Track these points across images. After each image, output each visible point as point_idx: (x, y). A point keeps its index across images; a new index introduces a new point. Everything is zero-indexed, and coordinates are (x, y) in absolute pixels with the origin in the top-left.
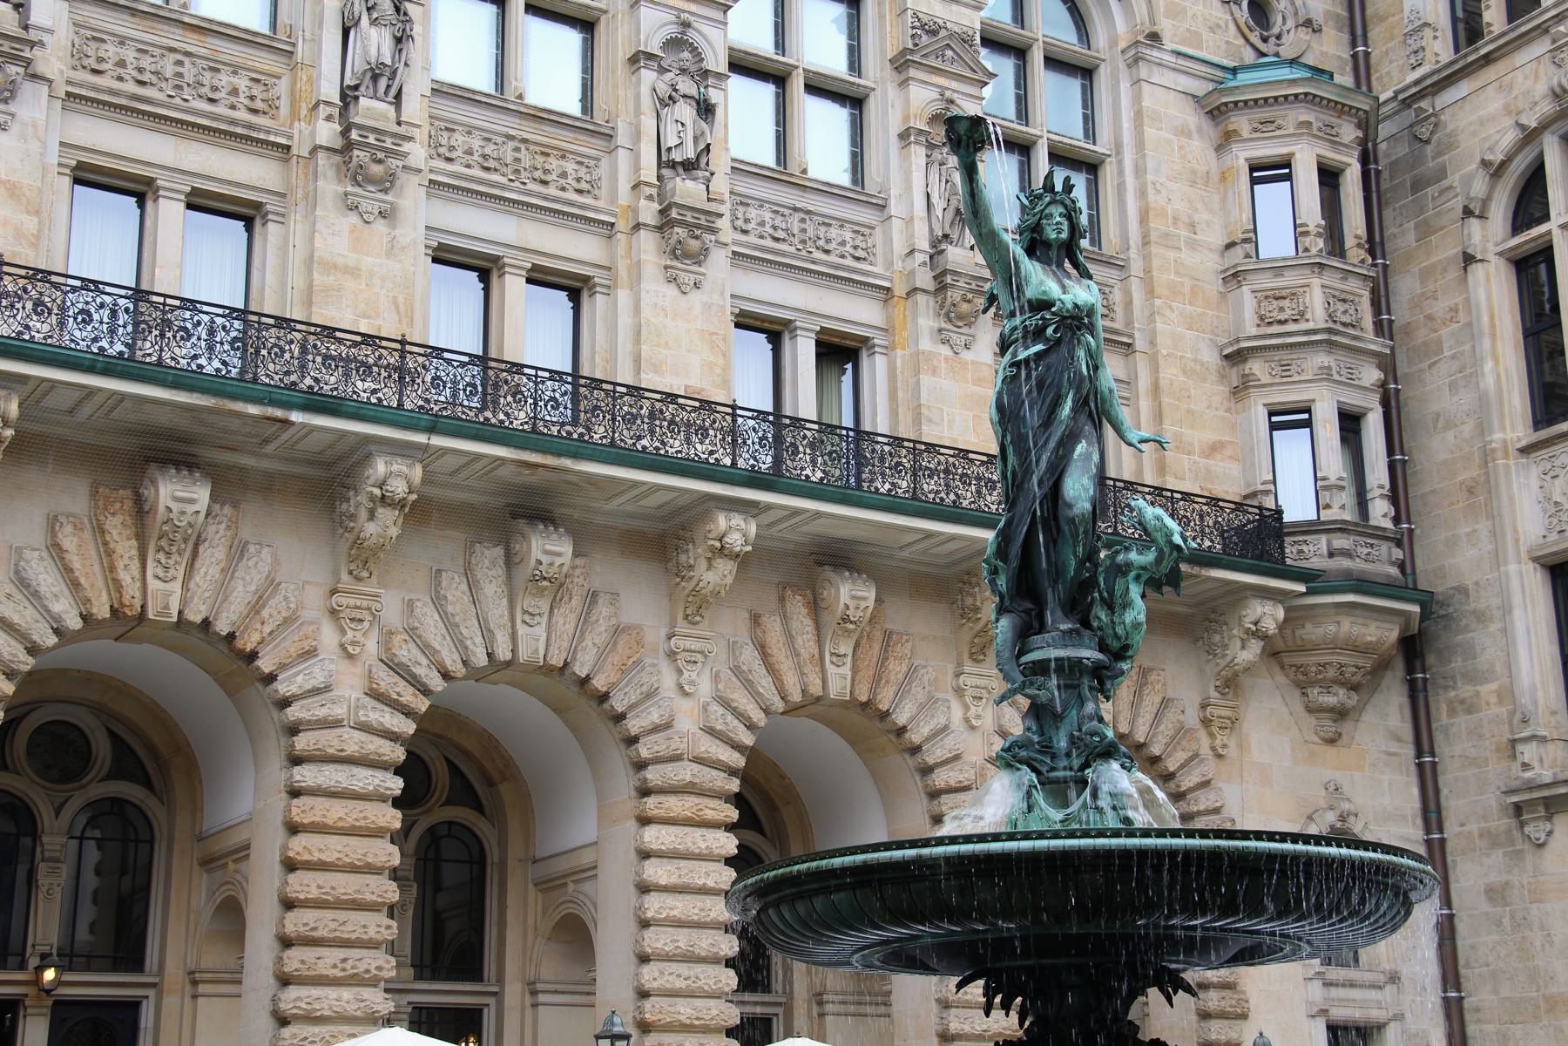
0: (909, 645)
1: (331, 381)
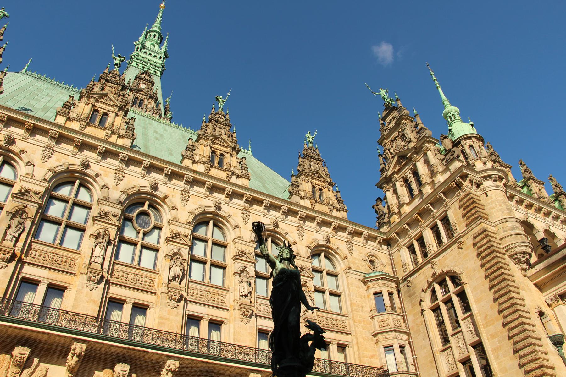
1: (159, 342)
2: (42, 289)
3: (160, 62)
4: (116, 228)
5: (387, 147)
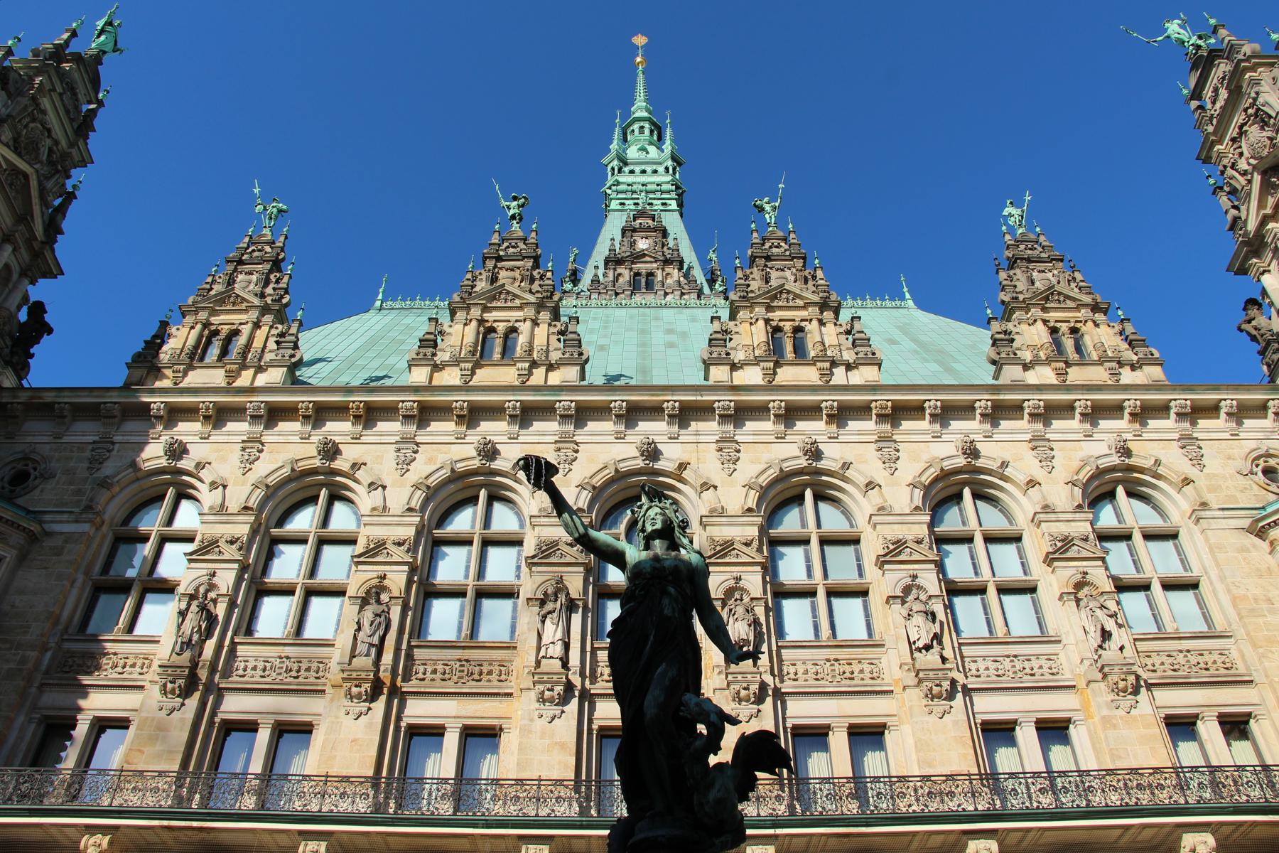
2: (451, 741)
3: (669, 178)
4: (759, 568)
5: (1225, 161)
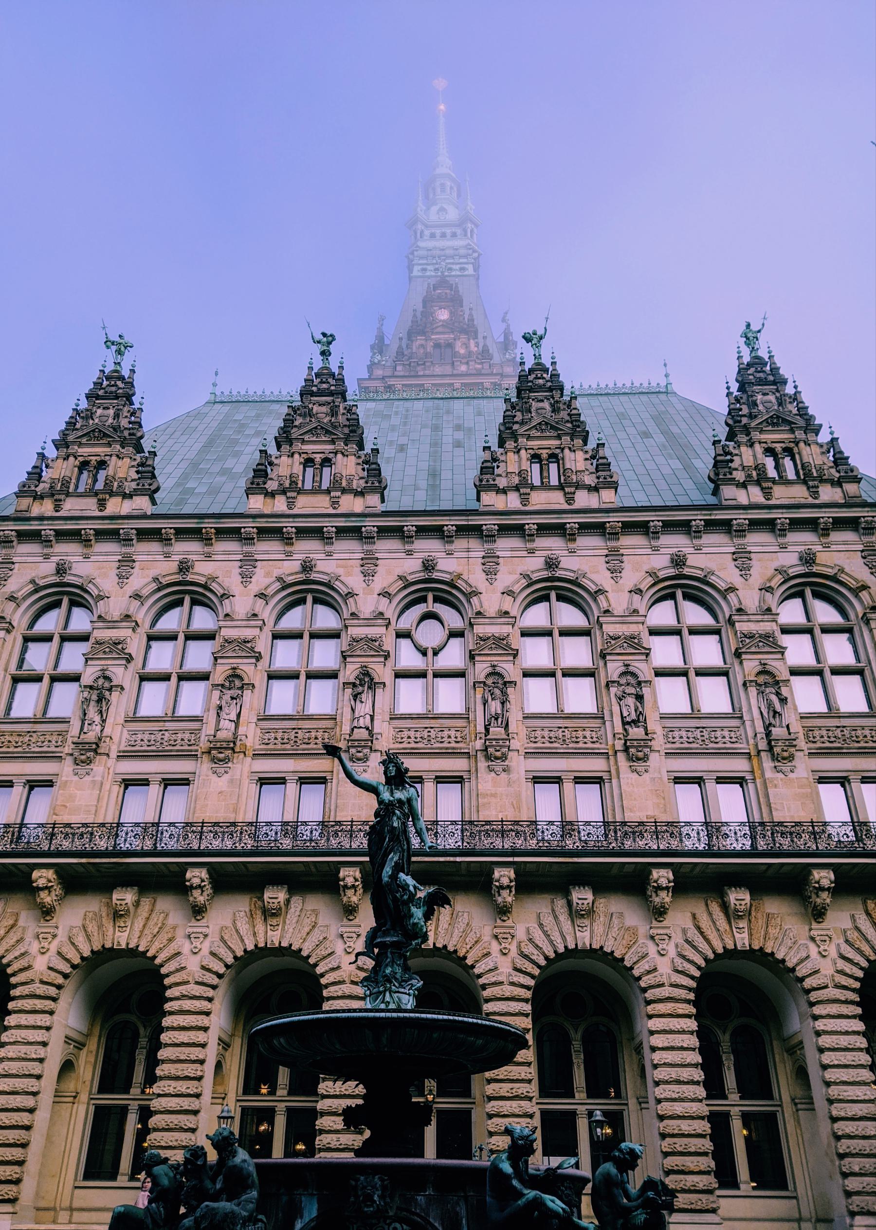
0: (779, 919)
